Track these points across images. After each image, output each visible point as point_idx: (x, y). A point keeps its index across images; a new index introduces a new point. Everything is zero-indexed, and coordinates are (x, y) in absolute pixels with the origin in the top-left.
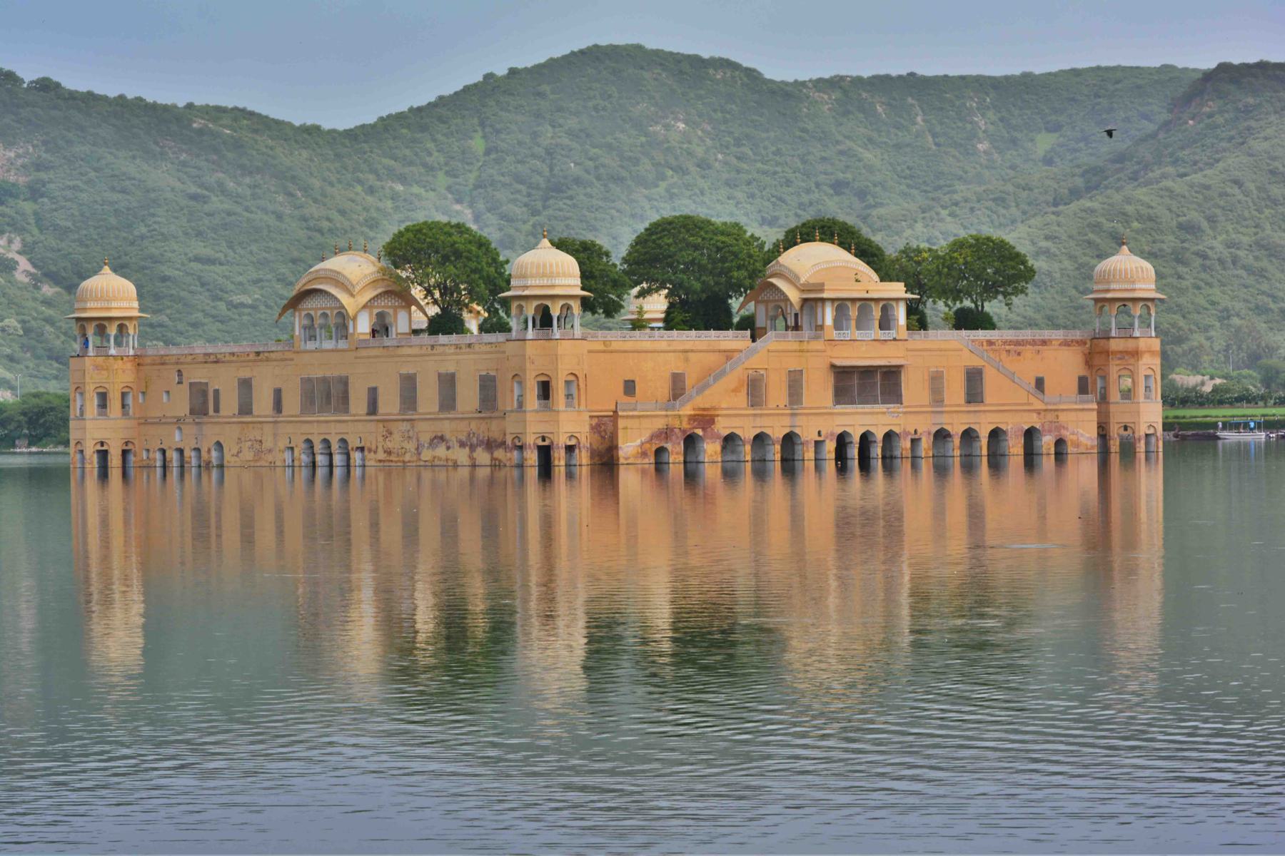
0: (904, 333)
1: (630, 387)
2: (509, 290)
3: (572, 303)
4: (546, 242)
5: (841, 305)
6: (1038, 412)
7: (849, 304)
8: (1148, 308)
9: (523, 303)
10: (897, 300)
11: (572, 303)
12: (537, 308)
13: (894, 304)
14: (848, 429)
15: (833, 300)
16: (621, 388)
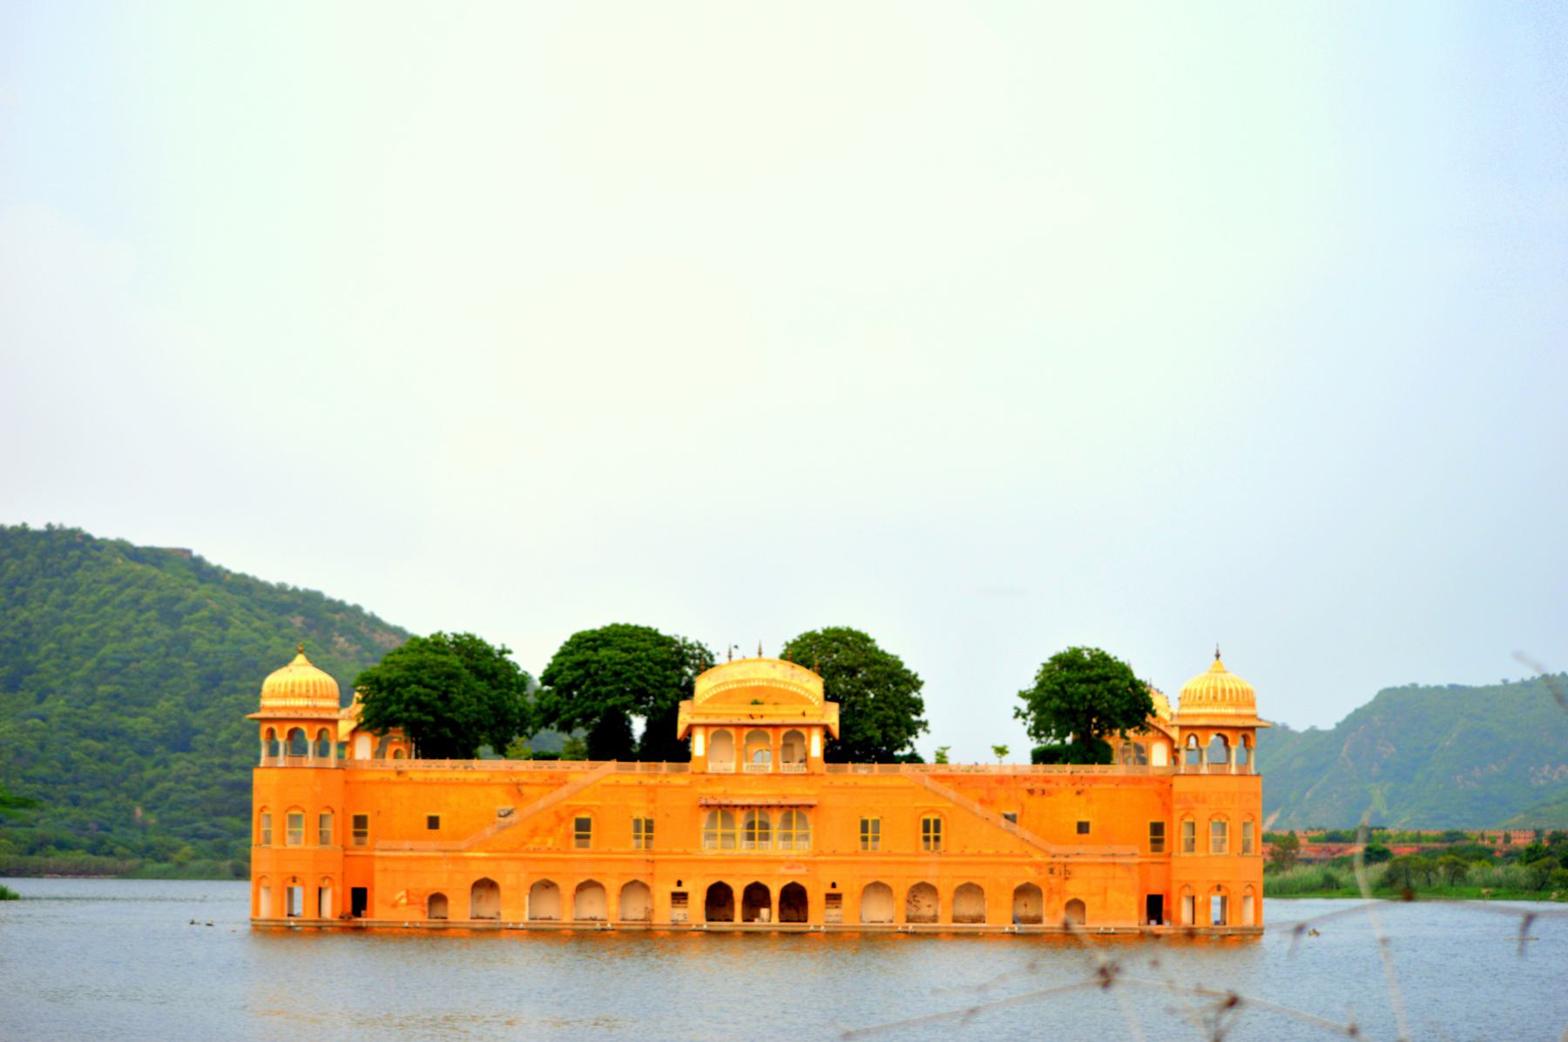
0: (823, 767)
1: (433, 823)
2: (259, 710)
3: (304, 727)
4: (300, 659)
5: (719, 731)
6: (1037, 866)
7: (732, 731)
8: (1226, 739)
9: (274, 726)
10: (809, 726)
11: (304, 727)
12: (292, 733)
13: (804, 731)
14: (728, 881)
15: (706, 726)
16: (425, 823)
